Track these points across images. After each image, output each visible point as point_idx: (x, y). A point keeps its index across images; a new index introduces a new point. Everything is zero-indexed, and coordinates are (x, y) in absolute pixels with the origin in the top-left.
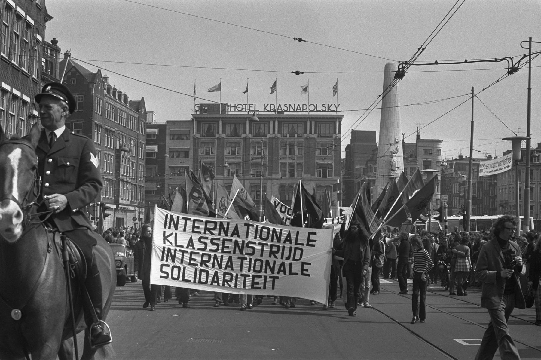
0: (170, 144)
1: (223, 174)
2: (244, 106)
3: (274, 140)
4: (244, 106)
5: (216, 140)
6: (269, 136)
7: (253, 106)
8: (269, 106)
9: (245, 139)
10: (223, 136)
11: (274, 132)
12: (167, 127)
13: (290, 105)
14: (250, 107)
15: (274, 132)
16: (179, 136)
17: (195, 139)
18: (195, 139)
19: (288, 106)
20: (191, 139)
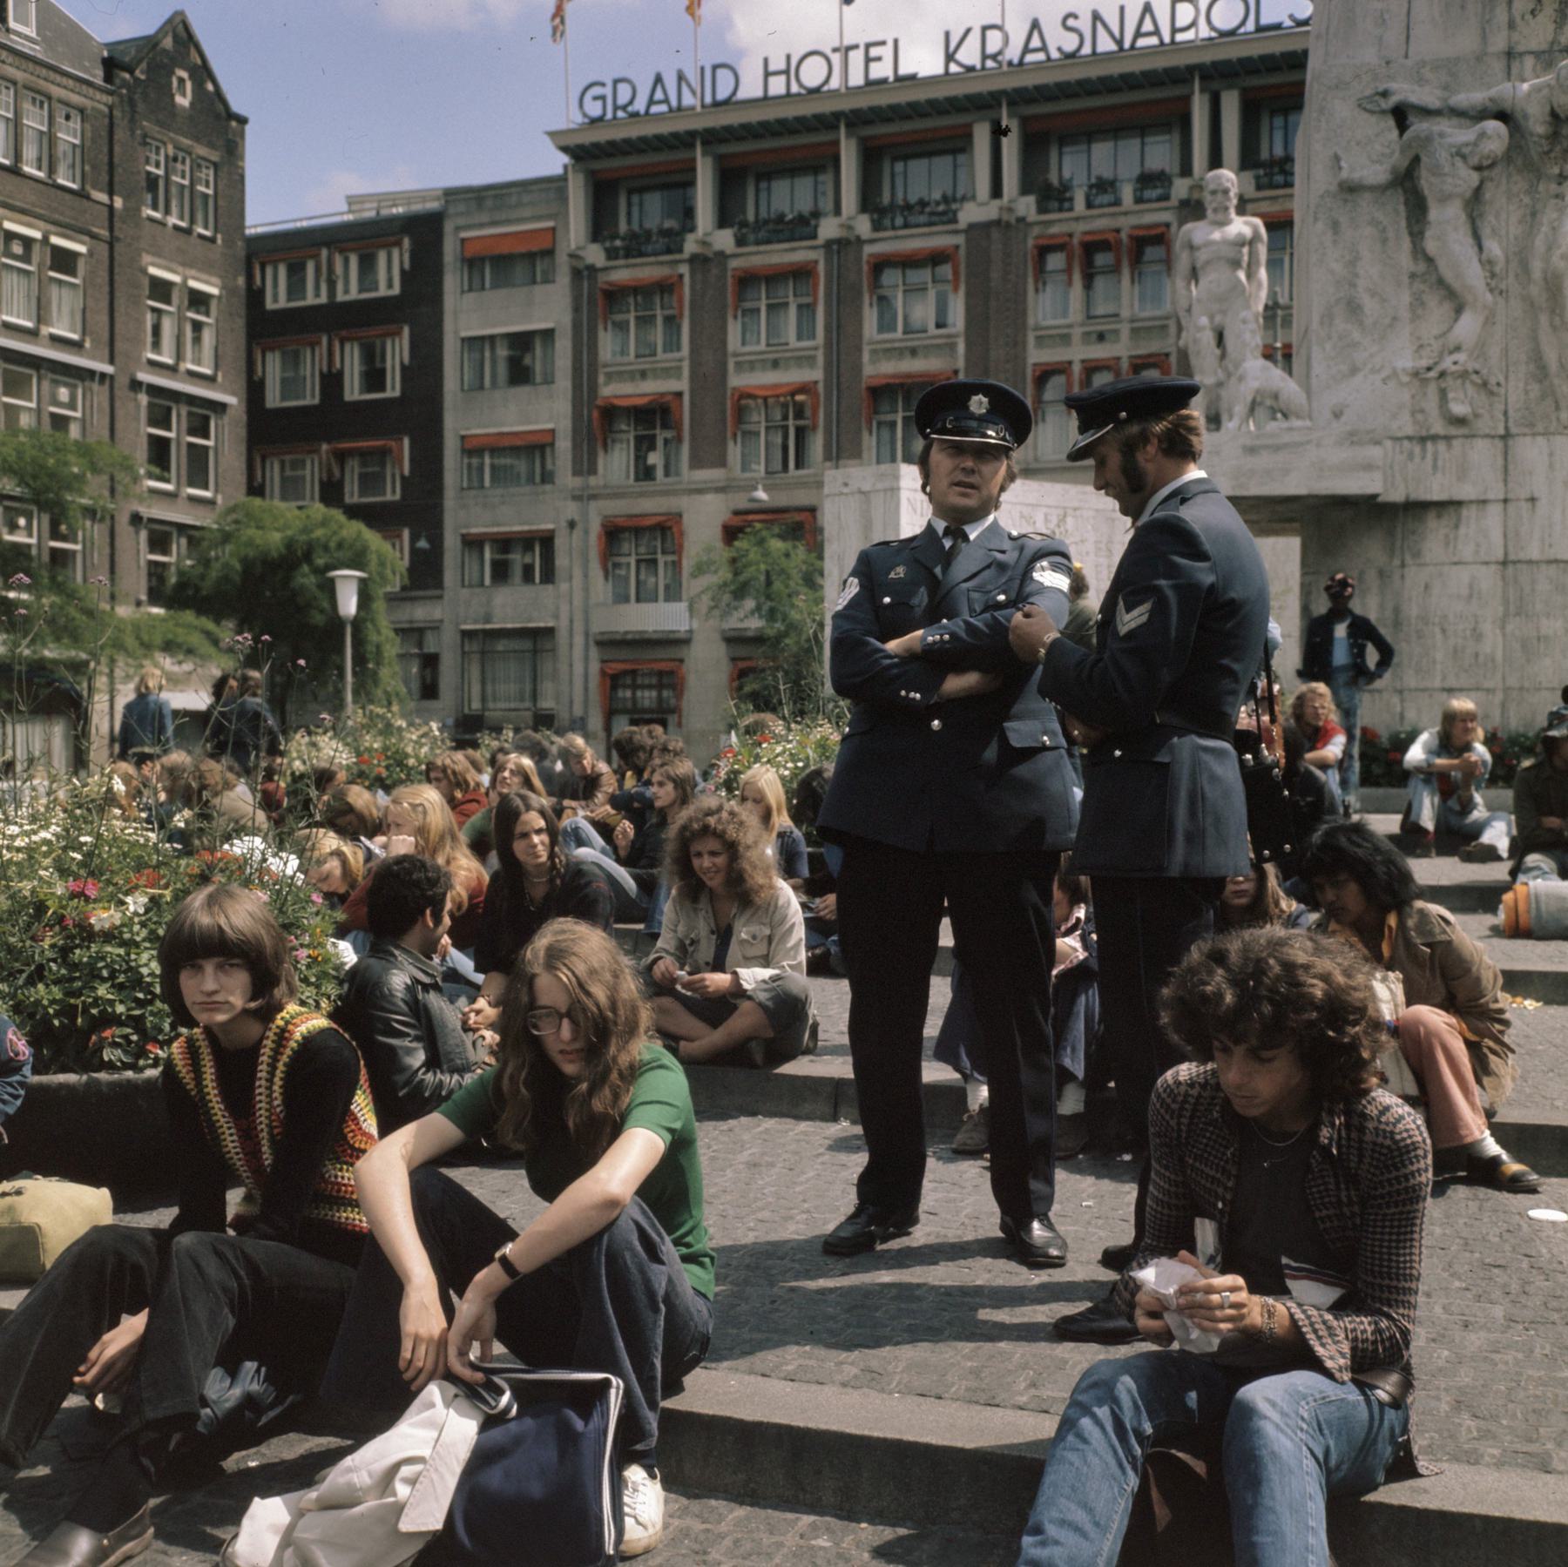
0: (469, 314)
1: (722, 462)
2: (836, 59)
3: (995, 234)
4: (836, 59)
5: (684, 269)
6: (970, 214)
7: (886, 52)
8: (974, 40)
9: (842, 247)
10: (718, 246)
11: (996, 191)
12: (448, 227)
13: (1096, 17)
14: (868, 60)
15: (996, 191)
16: (505, 265)
17: (582, 273)
18: (582, 273)
19: (1084, 24)
20: (563, 279)
